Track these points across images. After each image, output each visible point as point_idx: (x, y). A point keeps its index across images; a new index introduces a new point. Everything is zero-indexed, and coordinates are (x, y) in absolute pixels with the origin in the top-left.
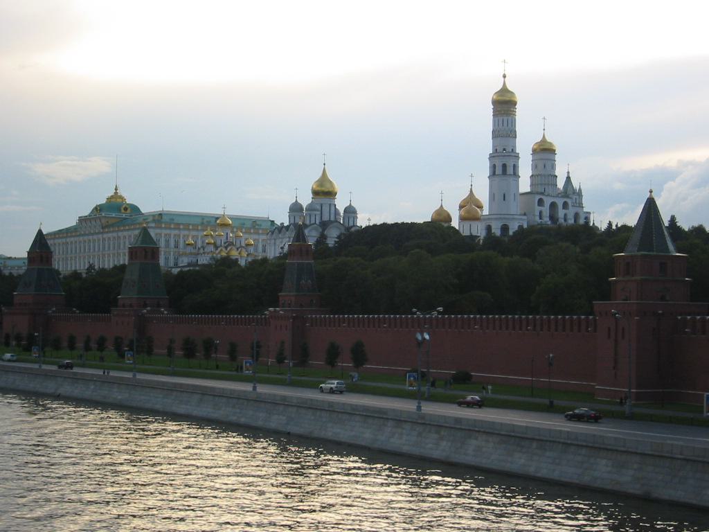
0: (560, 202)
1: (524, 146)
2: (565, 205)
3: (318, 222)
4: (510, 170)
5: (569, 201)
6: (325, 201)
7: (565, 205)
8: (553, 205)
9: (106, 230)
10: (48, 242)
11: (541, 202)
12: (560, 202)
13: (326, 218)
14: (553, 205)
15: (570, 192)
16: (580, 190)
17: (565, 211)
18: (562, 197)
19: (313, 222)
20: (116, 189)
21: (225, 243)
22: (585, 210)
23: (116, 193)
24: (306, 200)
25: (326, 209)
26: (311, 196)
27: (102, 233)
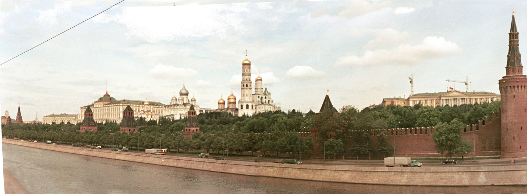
0: (264, 97)
1: (253, 78)
2: (265, 98)
3: (182, 104)
4: (249, 86)
5: (267, 96)
6: (185, 97)
7: (265, 98)
8: (262, 98)
9: (105, 106)
10: (91, 109)
11: (259, 97)
12: (264, 97)
13: (185, 102)
14: (262, 98)
15: (267, 93)
16: (270, 93)
17: (265, 100)
18: (264, 95)
19: (181, 103)
20: (107, 92)
21: (147, 110)
22: (272, 99)
23: (107, 94)
24: (178, 96)
25: (185, 99)
26: (179, 95)
27: (103, 107)
